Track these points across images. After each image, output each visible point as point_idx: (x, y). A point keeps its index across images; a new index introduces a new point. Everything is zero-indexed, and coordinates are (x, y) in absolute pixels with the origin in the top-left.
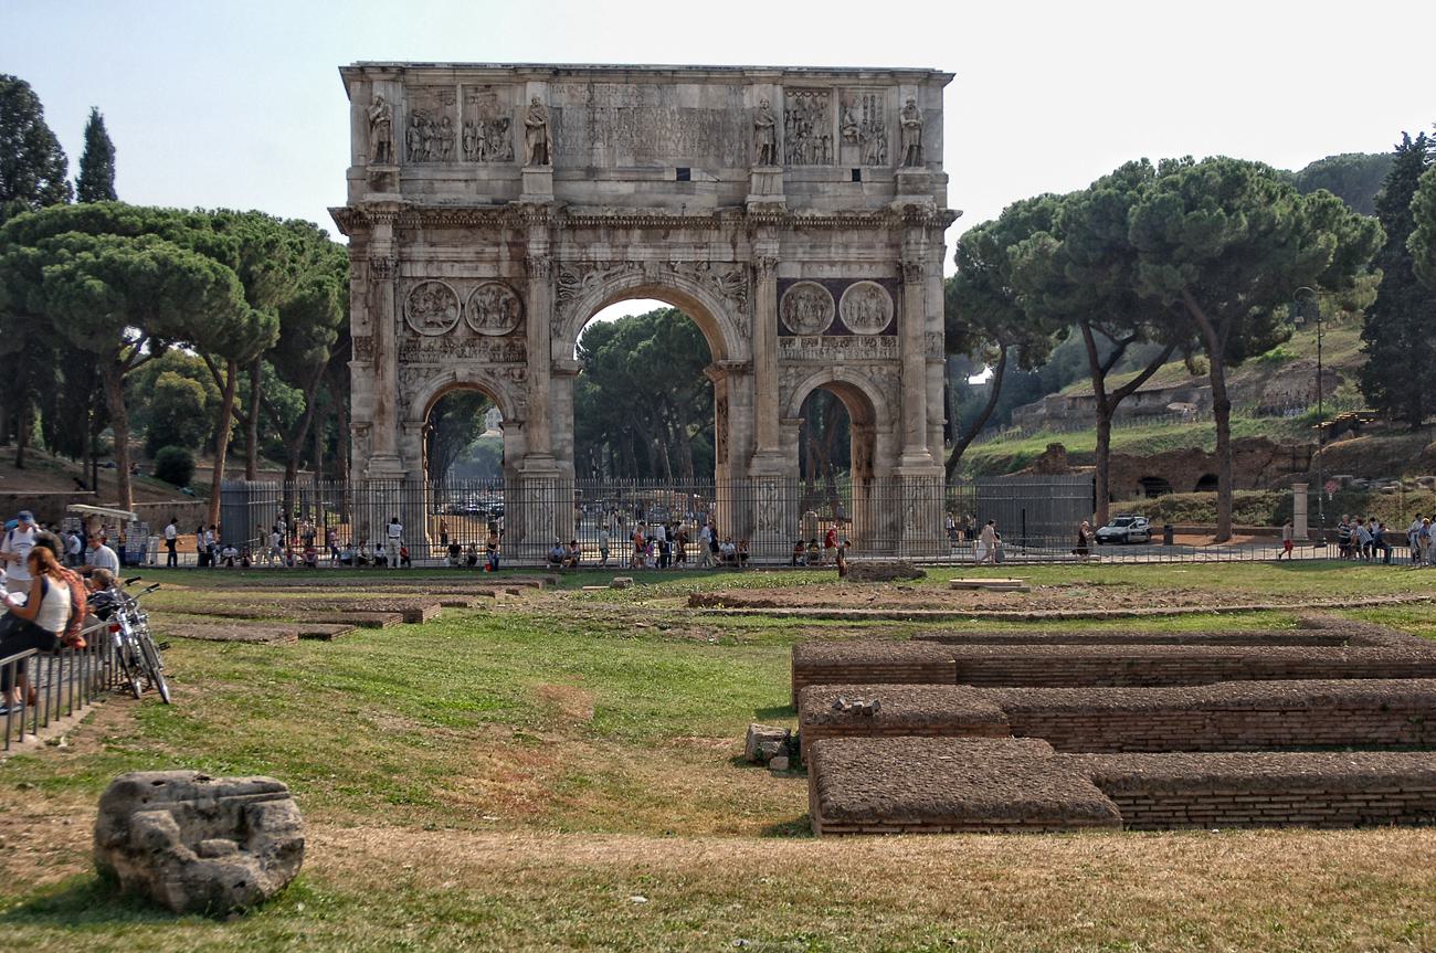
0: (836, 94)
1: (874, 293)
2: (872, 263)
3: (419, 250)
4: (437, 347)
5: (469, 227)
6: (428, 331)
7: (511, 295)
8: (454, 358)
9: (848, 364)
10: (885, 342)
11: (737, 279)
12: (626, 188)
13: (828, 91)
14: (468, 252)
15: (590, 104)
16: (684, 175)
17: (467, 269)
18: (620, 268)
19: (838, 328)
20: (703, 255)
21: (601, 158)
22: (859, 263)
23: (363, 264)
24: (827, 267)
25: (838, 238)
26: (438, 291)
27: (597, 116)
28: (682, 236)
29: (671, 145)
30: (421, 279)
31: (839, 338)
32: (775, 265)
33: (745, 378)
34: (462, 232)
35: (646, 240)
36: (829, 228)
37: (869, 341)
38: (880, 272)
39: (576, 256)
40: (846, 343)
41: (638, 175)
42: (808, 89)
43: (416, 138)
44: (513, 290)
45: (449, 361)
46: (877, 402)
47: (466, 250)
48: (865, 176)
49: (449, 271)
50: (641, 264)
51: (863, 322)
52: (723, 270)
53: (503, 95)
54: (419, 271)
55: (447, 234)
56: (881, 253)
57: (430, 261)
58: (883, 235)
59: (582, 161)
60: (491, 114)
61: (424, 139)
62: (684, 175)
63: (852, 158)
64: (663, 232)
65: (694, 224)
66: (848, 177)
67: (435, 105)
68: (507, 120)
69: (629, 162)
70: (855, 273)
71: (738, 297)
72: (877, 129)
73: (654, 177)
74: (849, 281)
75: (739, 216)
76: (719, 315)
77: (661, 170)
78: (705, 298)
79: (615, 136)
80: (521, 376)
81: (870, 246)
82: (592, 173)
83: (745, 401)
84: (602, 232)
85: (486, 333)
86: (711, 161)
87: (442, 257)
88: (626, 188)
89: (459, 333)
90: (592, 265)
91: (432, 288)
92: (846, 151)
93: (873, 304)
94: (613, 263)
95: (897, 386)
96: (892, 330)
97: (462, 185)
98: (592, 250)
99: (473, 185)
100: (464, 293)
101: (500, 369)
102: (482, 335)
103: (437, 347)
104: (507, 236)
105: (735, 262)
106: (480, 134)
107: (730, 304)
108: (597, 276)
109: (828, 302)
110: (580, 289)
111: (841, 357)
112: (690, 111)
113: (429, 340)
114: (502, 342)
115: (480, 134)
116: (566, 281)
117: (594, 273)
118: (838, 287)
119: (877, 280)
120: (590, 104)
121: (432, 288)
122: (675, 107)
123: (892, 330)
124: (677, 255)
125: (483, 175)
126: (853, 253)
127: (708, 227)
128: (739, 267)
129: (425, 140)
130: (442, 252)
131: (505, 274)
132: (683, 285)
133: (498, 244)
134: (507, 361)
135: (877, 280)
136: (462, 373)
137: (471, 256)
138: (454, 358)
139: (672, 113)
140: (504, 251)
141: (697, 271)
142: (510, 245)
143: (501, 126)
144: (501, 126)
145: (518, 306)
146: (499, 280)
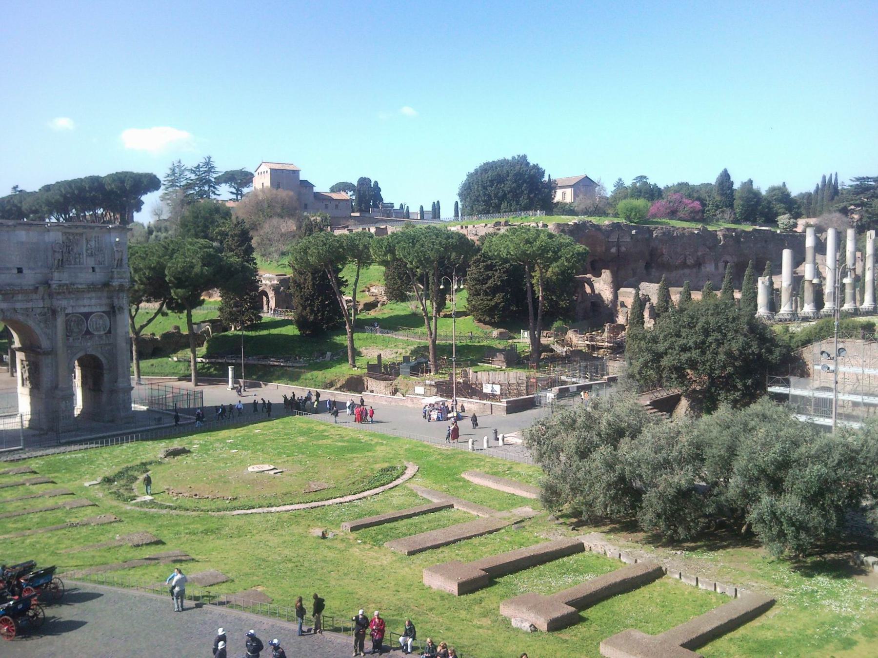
0: (84, 236)
1: (101, 317)
2: (101, 305)
9: (91, 347)
11: (45, 314)
13: (81, 234)
16: (20, 270)
19: (88, 332)
20: (30, 305)
28: (20, 297)
32: (65, 308)
37: (100, 337)
38: (104, 309)
48: (97, 270)
51: (97, 330)
52: (39, 311)
56: (105, 301)
58: (105, 294)
62: (20, 270)
63: (91, 262)
66: (91, 270)
70: (94, 309)
71: (46, 321)
74: (91, 313)
77: (8, 269)
78: (31, 323)
81: (100, 298)
92: (89, 259)
95: (113, 354)
96: (109, 332)
107: (42, 325)
112: (22, 243)
118: (87, 315)
123: (109, 332)
124: (18, 306)
126: (93, 301)
132: (21, 318)
141: (27, 312)
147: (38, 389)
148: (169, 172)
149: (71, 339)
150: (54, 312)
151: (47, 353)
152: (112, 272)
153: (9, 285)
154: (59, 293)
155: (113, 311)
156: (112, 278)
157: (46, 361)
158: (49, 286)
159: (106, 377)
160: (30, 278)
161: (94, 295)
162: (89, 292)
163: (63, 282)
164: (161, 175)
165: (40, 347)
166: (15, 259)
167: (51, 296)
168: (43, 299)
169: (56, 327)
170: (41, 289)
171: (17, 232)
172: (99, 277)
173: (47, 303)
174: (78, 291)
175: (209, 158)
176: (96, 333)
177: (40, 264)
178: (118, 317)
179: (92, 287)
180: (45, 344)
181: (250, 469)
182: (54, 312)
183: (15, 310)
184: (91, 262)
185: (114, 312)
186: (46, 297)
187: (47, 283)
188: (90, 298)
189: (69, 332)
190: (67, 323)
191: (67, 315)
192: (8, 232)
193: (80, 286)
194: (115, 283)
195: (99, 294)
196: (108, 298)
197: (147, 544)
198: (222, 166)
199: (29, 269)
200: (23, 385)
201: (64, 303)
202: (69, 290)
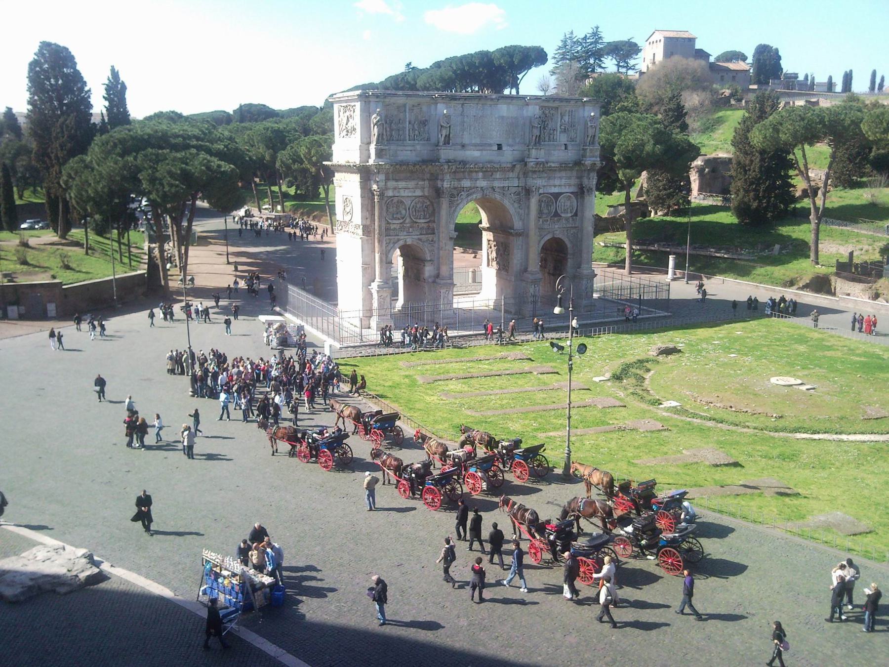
2: (570, 185)
3: (391, 184)
6: (395, 222)
11: (519, 194)
12: (477, 154)
14: (411, 184)
15: (462, 115)
16: (500, 147)
19: (556, 214)
21: (466, 141)
22: (565, 186)
25: (558, 174)
28: (498, 175)
29: (495, 133)
35: (484, 178)
37: (567, 219)
38: (573, 189)
40: (558, 221)
41: (482, 146)
42: (549, 108)
46: (569, 245)
48: (570, 147)
49: (403, 193)
51: (565, 211)
52: (513, 190)
53: (424, 108)
54: (390, 193)
56: (574, 181)
58: (574, 173)
59: (459, 141)
61: (391, 130)
62: (500, 147)
63: (563, 139)
65: (503, 170)
66: (563, 148)
67: (396, 113)
69: (478, 141)
71: (519, 201)
72: (572, 125)
74: (561, 194)
76: (512, 211)
77: (490, 145)
78: (507, 203)
81: (570, 178)
82: (463, 146)
85: (418, 221)
86: (510, 141)
88: (477, 154)
89: (407, 221)
90: (463, 189)
92: (562, 135)
93: (568, 203)
94: (471, 188)
96: (576, 214)
100: (408, 202)
106: (416, 126)
107: (516, 205)
112: (503, 117)
113: (395, 226)
114: (425, 226)
115: (416, 126)
116: (456, 197)
118: (557, 196)
121: (396, 199)
123: (576, 214)
124: (496, 184)
125: (418, 147)
126: (563, 181)
130: (402, 184)
132: (498, 197)
133: (424, 180)
136: (409, 242)
140: (427, 182)
142: (429, 180)
143: (424, 123)
144: (424, 123)
145: (431, 209)
147: (507, 271)
148: (560, 44)
150: (528, 192)
151: (519, 235)
152: (584, 150)
153: (490, 162)
154: (534, 172)
155: (581, 192)
156: (584, 156)
157: (517, 244)
159: (570, 262)
160: (509, 155)
161: (563, 174)
162: (560, 171)
164: (551, 49)
166: (496, 135)
167: (525, 174)
168: (519, 178)
169: (529, 207)
170: (518, 166)
171: (499, 106)
172: (570, 155)
174: (552, 170)
175: (597, 28)
176: (563, 215)
177: (517, 140)
178: (587, 198)
179: (564, 167)
180: (518, 224)
181: (774, 380)
182: (528, 192)
183: (493, 188)
184: (563, 139)
185: (582, 193)
186: (521, 176)
187: (523, 161)
188: (561, 178)
189: (540, 213)
190: (540, 201)
192: (491, 105)
195: (569, 173)
196: (578, 178)
197: (726, 465)
198: (609, 36)
199: (509, 145)
200: (488, 265)
201: (539, 182)
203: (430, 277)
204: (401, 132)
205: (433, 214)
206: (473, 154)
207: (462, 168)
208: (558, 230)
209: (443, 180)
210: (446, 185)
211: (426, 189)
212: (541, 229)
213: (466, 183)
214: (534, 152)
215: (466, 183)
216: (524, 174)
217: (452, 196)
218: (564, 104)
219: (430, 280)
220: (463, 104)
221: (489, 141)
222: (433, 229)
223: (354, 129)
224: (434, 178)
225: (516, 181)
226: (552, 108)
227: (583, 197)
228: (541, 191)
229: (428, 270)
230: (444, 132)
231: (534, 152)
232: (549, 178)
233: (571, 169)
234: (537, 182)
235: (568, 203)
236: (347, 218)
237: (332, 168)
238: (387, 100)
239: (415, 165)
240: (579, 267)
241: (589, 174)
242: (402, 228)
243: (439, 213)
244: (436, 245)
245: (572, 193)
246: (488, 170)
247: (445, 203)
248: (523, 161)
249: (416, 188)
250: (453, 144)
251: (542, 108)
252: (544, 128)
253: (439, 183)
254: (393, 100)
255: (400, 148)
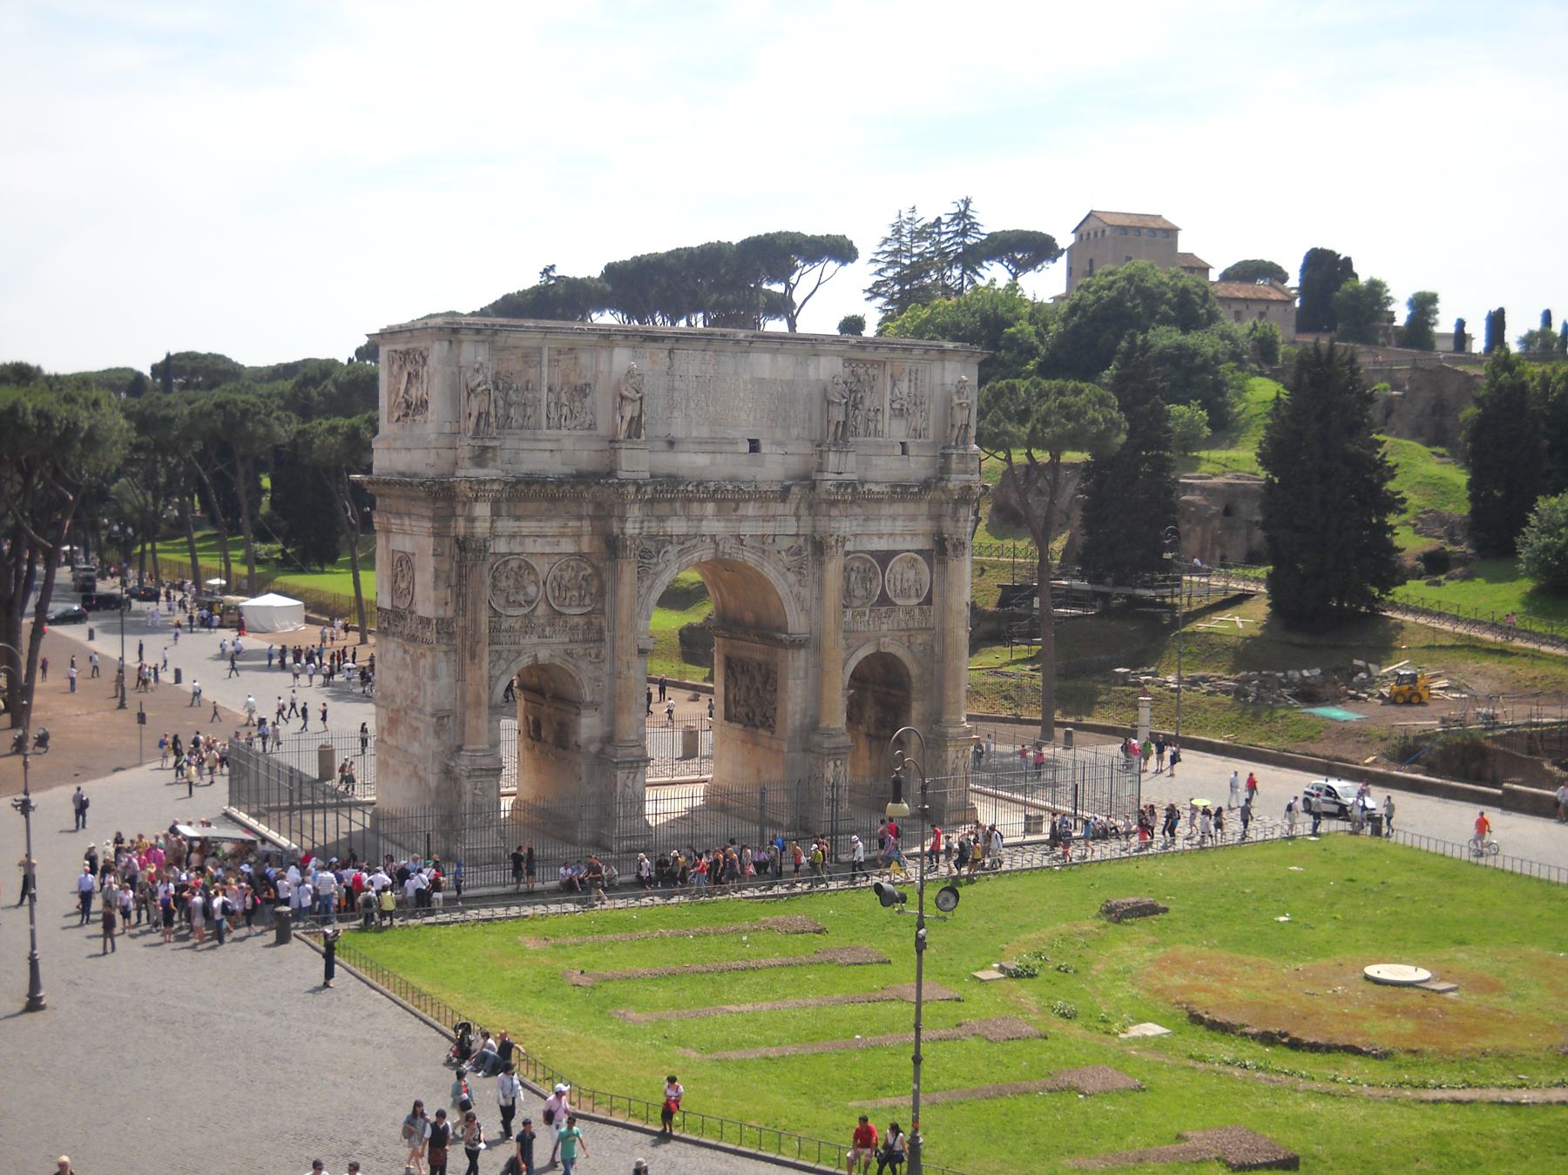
0: (888, 367)
3: (506, 525)
4: (517, 626)
5: (553, 499)
6: (510, 611)
7: (589, 571)
8: (535, 639)
10: (922, 612)
11: (799, 552)
12: (702, 460)
13: (882, 364)
14: (551, 527)
15: (670, 372)
16: (754, 446)
17: (549, 543)
18: (694, 542)
19: (884, 600)
20: (769, 528)
21: (678, 431)
23: (447, 541)
24: (876, 539)
25: (887, 510)
26: (520, 567)
27: (677, 384)
28: (751, 509)
30: (503, 555)
31: (883, 609)
33: (803, 652)
34: (545, 505)
35: (719, 514)
36: (879, 501)
37: (909, 611)
38: (922, 543)
39: (654, 530)
41: (713, 444)
42: (864, 362)
43: (501, 403)
44: (593, 566)
45: (529, 640)
46: (914, 670)
47: (549, 524)
48: (912, 450)
49: (532, 546)
50: (713, 537)
51: (904, 593)
52: (786, 543)
53: (585, 359)
54: (501, 546)
55: (531, 506)
56: (924, 526)
57: (513, 536)
59: (661, 431)
60: (573, 378)
61: (508, 404)
62: (754, 446)
63: (896, 430)
64: (733, 505)
65: (762, 497)
66: (898, 450)
67: (518, 367)
68: (587, 385)
69: (705, 432)
70: (899, 545)
72: (918, 402)
73: (728, 448)
74: (891, 554)
75: (805, 487)
76: (782, 589)
77: (733, 442)
78: (770, 572)
79: (692, 405)
80: (597, 656)
81: (913, 518)
82: (671, 443)
83: (802, 674)
84: (678, 505)
85: (567, 611)
86: (779, 434)
87: (525, 531)
88: (702, 460)
91: (514, 564)
92: (895, 423)
93: (911, 575)
94: (687, 537)
95: (936, 658)
96: (928, 601)
97: (548, 454)
98: (669, 524)
99: (558, 456)
100: (542, 568)
101: (579, 649)
102: (561, 614)
103: (517, 626)
104: (588, 509)
105: (797, 535)
106: (564, 399)
107: (792, 577)
108: (672, 550)
109: (876, 573)
110: (656, 564)
111: (884, 627)
112: (761, 381)
113: (511, 621)
114: (581, 621)
115: (564, 399)
117: (669, 548)
118: (885, 558)
119: (917, 552)
120: (670, 372)
121: (514, 564)
122: (747, 377)
123: (928, 601)
124: (747, 529)
125: (568, 444)
127: (775, 500)
128: (801, 541)
129: (510, 405)
130: (528, 526)
131: (586, 549)
132: (750, 558)
133: (580, 518)
134: (586, 641)
135: (917, 552)
136: (543, 655)
137: (555, 531)
138: (535, 639)
139: (745, 382)
140: (586, 525)
142: (592, 518)
143: (582, 391)
144: (582, 391)
145: (595, 583)
146: (580, 555)
149: (849, 612)
150: (819, 547)
151: (797, 644)
152: (946, 457)
153: (732, 480)
154: (834, 503)
155: (940, 550)
156: (944, 470)
158: (813, 486)
159: (917, 709)
160: (773, 467)
161: (898, 508)
162: (892, 501)
163: (845, 476)
164: (868, 241)
165: (782, 628)
166: (746, 423)
168: (798, 517)
169: (821, 583)
170: (795, 490)
171: (753, 357)
172: (916, 467)
173: (806, 529)
175: (967, 203)
176: (899, 602)
177: (794, 432)
178: (952, 564)
179: (901, 491)
180: (796, 623)
183: (739, 539)
184: (896, 430)
186: (803, 511)
188: (894, 518)
189: (848, 593)
190: (847, 570)
191: (847, 553)
193: (875, 488)
194: (955, 482)
195: (911, 508)
196: (931, 518)
198: (992, 220)
201: (845, 526)
202: (854, 494)
203: (591, 740)
204: (529, 411)
205: (601, 592)
206: (691, 462)
207: (669, 490)
208: (886, 635)
209: (623, 519)
210: (631, 528)
211: (585, 540)
212: (848, 632)
213: (677, 526)
214: (832, 459)
215: (677, 526)
216: (810, 507)
217: (645, 554)
218: (899, 354)
219: (593, 748)
220: (671, 351)
221: (732, 433)
222: (601, 631)
223: (424, 404)
224: (604, 514)
225: (792, 522)
226: (873, 362)
227: (943, 563)
228: (849, 546)
229: (588, 726)
230: (629, 411)
231: (832, 459)
232: (867, 519)
233: (917, 498)
234: (844, 525)
235: (911, 575)
236: (402, 605)
237: (370, 489)
238: (500, 339)
239: (560, 482)
240: (938, 721)
241: (955, 512)
242: (528, 628)
243: (615, 593)
244: (607, 667)
245: (919, 552)
246: (728, 496)
247: (628, 571)
248: (808, 481)
249: (562, 535)
250: (648, 439)
251: (849, 361)
252: (855, 407)
253: (615, 527)
254: (513, 339)
255: (525, 445)
